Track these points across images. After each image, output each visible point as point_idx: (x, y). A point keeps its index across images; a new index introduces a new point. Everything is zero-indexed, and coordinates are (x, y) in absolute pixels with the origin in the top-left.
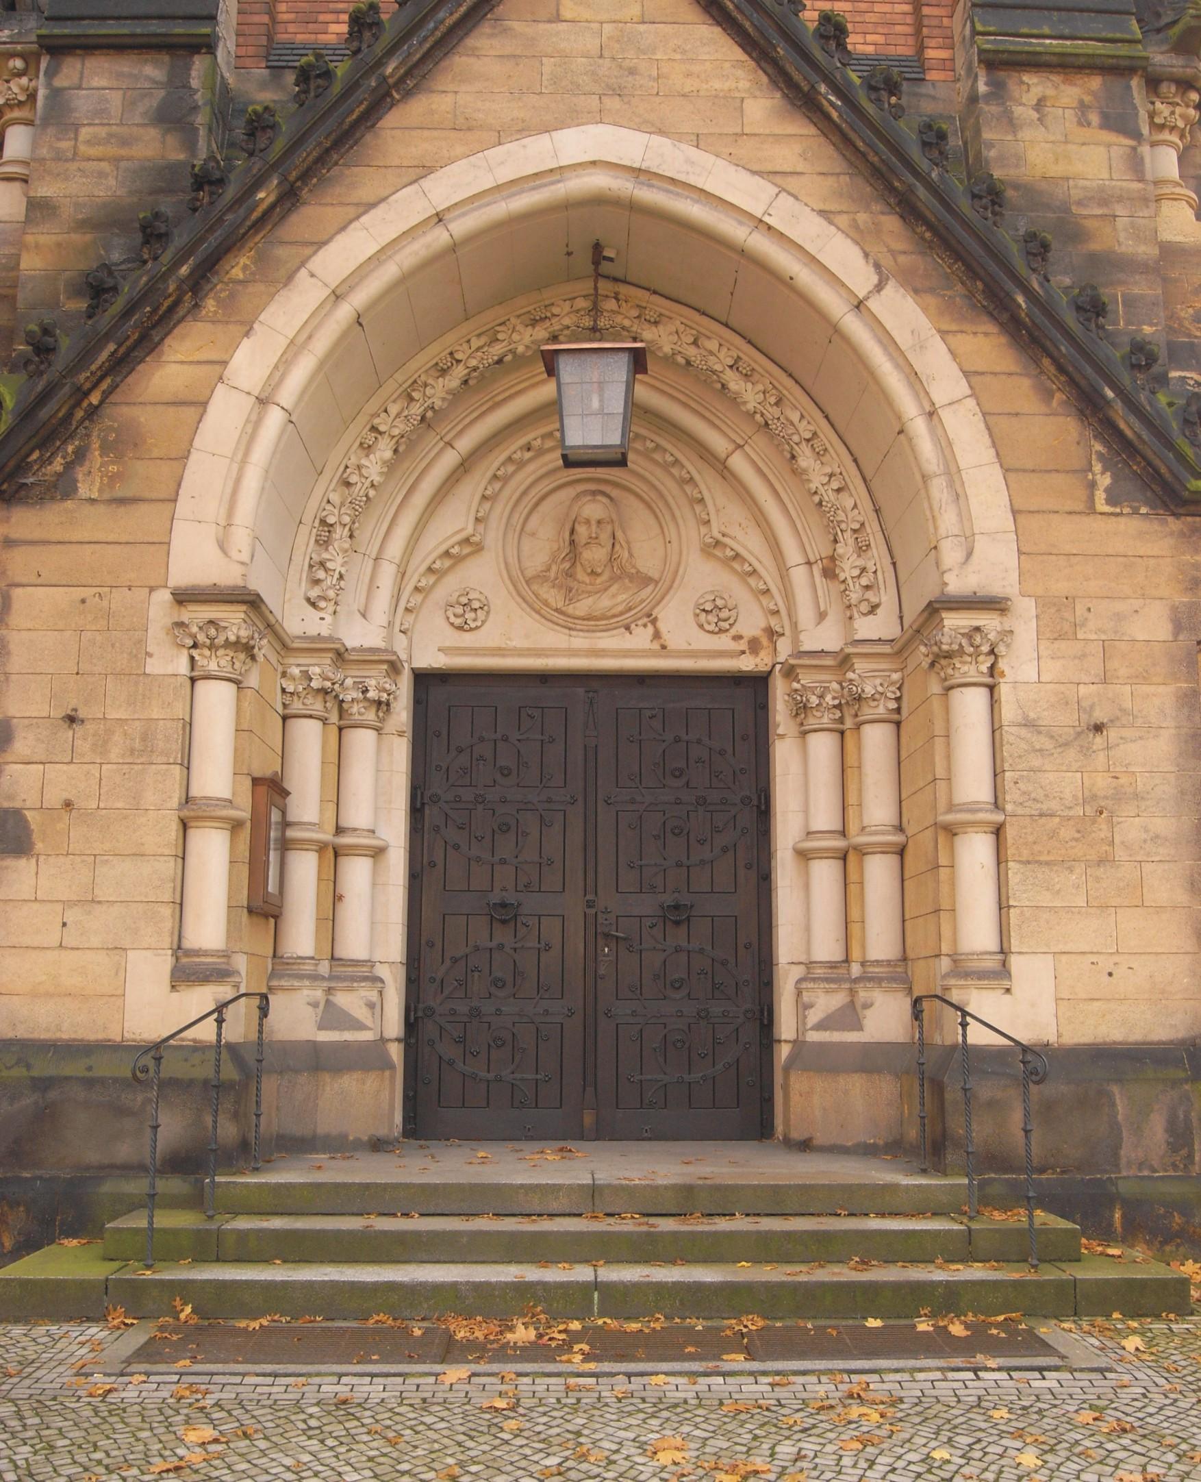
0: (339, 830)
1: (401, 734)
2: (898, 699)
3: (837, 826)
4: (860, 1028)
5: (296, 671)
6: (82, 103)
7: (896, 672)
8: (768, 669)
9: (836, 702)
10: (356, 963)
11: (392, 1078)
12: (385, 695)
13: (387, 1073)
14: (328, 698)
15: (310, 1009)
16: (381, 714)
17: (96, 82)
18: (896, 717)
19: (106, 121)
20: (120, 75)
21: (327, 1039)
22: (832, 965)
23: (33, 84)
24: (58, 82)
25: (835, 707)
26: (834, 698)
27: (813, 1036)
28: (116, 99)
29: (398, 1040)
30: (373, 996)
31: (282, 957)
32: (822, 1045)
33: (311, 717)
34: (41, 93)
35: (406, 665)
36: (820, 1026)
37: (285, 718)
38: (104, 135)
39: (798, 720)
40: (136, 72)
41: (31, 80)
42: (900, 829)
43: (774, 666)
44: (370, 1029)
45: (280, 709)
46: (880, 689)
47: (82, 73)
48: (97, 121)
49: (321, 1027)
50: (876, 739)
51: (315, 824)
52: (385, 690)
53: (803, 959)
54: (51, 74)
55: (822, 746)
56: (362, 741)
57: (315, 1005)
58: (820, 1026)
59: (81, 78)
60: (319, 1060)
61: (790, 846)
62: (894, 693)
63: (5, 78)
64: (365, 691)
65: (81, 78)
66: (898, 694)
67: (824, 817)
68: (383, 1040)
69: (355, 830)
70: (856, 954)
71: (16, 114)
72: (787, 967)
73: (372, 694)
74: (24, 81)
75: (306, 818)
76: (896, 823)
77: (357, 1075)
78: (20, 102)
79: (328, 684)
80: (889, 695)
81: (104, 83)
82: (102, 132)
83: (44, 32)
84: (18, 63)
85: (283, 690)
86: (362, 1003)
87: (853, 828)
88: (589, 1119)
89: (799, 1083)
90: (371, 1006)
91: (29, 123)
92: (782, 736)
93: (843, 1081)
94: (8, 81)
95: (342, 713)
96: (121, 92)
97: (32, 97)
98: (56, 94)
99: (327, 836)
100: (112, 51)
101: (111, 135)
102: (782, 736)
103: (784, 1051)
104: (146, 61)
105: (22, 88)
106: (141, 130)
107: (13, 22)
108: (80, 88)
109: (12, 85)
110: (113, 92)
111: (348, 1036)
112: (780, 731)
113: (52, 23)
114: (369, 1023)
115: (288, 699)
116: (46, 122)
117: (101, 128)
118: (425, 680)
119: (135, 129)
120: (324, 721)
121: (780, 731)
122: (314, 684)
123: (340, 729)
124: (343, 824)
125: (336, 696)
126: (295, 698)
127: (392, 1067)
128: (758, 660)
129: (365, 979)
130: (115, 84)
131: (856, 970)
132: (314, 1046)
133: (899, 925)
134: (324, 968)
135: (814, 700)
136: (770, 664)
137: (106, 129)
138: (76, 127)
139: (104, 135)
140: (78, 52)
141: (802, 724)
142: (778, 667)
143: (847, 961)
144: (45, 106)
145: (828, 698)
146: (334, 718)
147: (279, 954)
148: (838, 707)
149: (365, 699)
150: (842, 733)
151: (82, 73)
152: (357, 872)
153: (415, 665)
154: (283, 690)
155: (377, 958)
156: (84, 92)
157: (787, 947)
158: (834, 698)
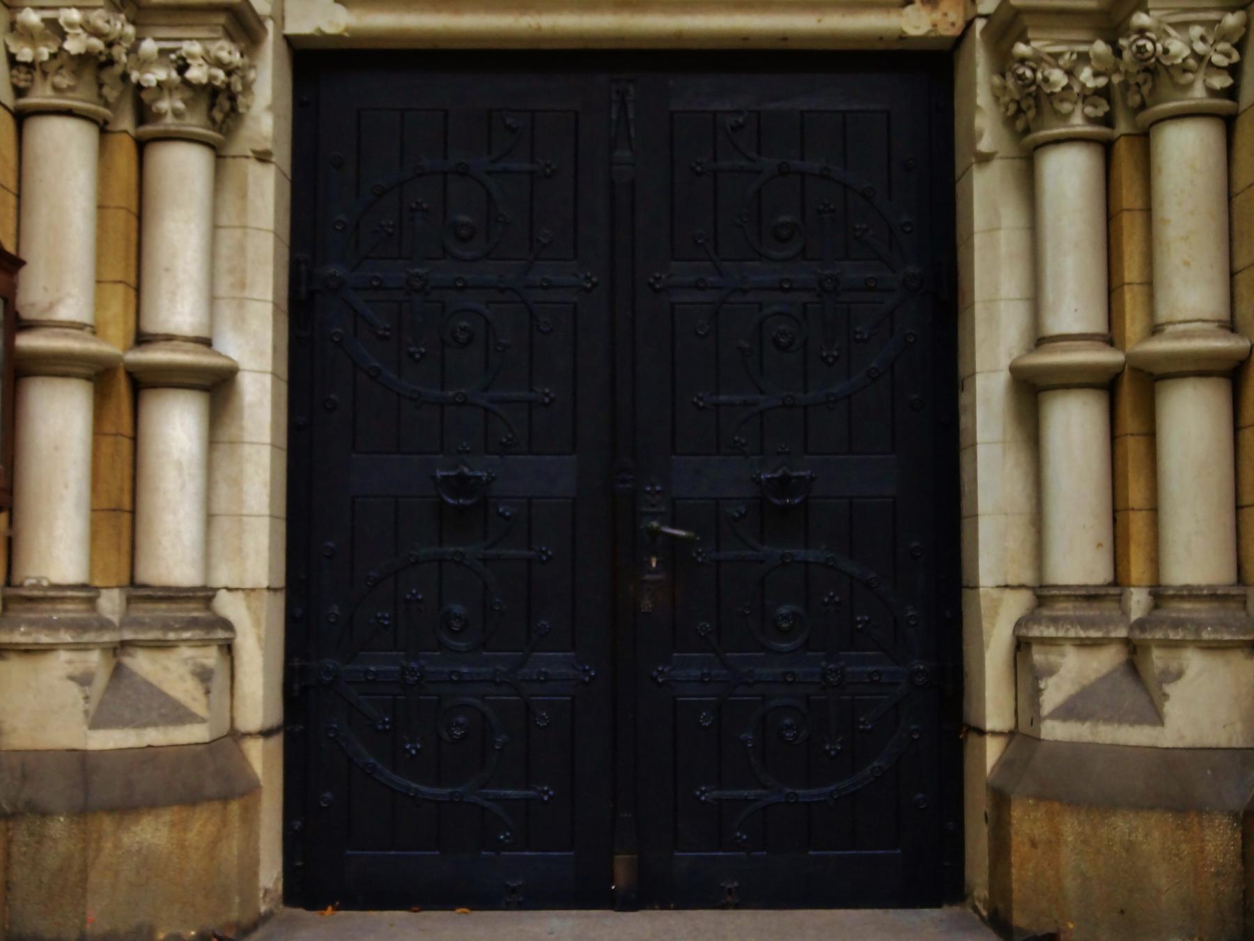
0: (142, 339)
1: (263, 157)
2: (1234, 70)
3: (1094, 322)
4: (1156, 717)
5: (32, 18)
7: (1232, 10)
8: (954, 32)
9: (1102, 81)
10: (174, 595)
11: (249, 818)
12: (221, 74)
13: (235, 807)
14: (106, 76)
15: (74, 690)
16: (218, 116)
18: (1226, 103)
21: (110, 745)
22: (1090, 596)
25: (1098, 92)
26: (1096, 74)
27: (1054, 731)
29: (266, 733)
30: (211, 657)
31: (21, 586)
32: (1076, 748)
33: (68, 113)
35: (270, 25)
36: (1067, 711)
37: (21, 117)
39: (1020, 124)
42: (1231, 326)
43: (969, 24)
44: (203, 721)
45: (9, 100)
46: (1200, 47)
49: (97, 722)
50: (1185, 151)
51: (81, 326)
52: (219, 63)
53: (1027, 577)
55: (1069, 174)
56: (183, 169)
57: (84, 680)
58: (1067, 711)
60: (100, 790)
61: (1005, 362)
62: (1228, 55)
64: (183, 67)
66: (1236, 57)
67: (1074, 307)
68: (236, 735)
69: (169, 338)
70: (1138, 569)
72: (996, 593)
73: (197, 73)
75: (65, 313)
76: (1224, 314)
77: (167, 816)
79: (98, 44)
80: (1217, 59)
85: (12, 61)
86: (184, 670)
87: (1133, 325)
88: (623, 871)
89: (1026, 821)
90: (204, 676)
92: (985, 159)
93: (1122, 825)
95: (143, 113)
99: (112, 346)
102: (985, 159)
103: (993, 750)
111: (154, 736)
112: (984, 145)
114: (199, 708)
115: (22, 79)
118: (312, 62)
120: (104, 129)
121: (984, 145)
122: (73, 46)
123: (142, 146)
124: (150, 327)
125: (125, 77)
126: (37, 75)
127: (251, 790)
128: (937, 16)
129: (192, 624)
131: (1138, 602)
132: (83, 760)
133: (1228, 518)
134: (111, 603)
135: (1058, 78)
136: (960, 23)
141: (1027, 131)
142: (980, 24)
143: (1119, 580)
145: (1086, 74)
146: (126, 123)
147: (16, 580)
148: (1104, 93)
149: (186, 83)
150: (1107, 148)
152: (177, 425)
153: (292, 28)
154: (12, 61)
155: (222, 577)
157: (995, 552)
158: (1096, 74)
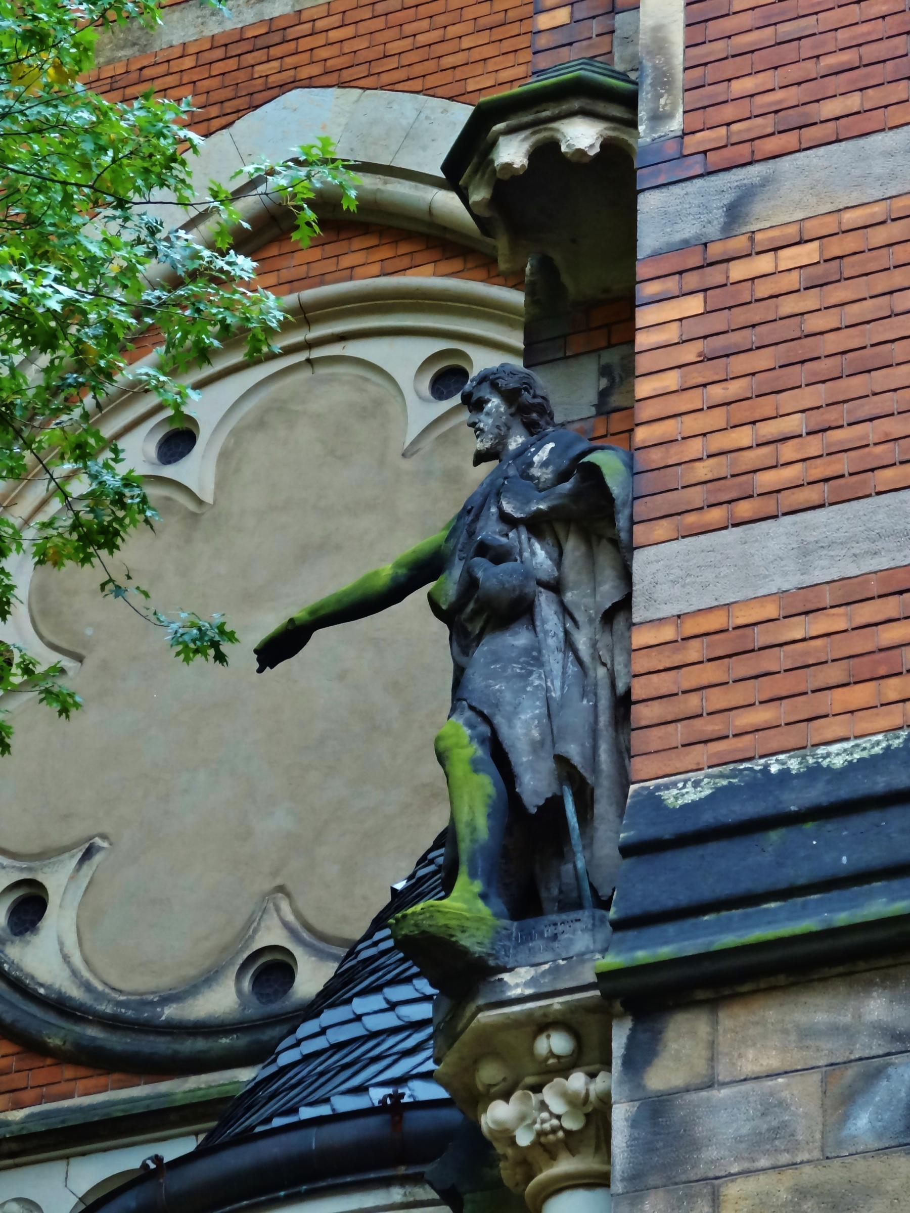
6: (723, 1124)
17: (753, 1061)
19: (785, 1158)
23: (599, 1084)
24: (660, 1077)
28: (802, 1097)
34: (620, 1115)
38: (784, 1196)
40: (846, 1018)
41: (592, 1076)
47: (712, 1045)
48: (763, 1162)
54: (639, 1058)
59: (712, 1059)
63: (530, 1080)
65: (712, 1059)
71: (565, 1165)
74: (577, 1081)
78: (568, 1133)
81: (772, 1061)
82: (779, 1187)
83: (612, 961)
84: (558, 1043)
91: (598, 1181)
94: (537, 1089)
96: (815, 1078)
97: (597, 1116)
98: (656, 1110)
100: (782, 979)
101: (801, 1193)
104: (869, 985)
106: (877, 1166)
107: (538, 943)
108: (711, 1084)
109: (548, 1095)
110: (797, 1078)
113: (631, 934)
116: (639, 1184)
117: (773, 1176)
119: (860, 1165)
130: (796, 1059)
137: (789, 1178)
138: (713, 1185)
139: (784, 1196)
140: (700, 995)
144: (633, 1144)
151: (712, 1045)
156: (724, 1092)
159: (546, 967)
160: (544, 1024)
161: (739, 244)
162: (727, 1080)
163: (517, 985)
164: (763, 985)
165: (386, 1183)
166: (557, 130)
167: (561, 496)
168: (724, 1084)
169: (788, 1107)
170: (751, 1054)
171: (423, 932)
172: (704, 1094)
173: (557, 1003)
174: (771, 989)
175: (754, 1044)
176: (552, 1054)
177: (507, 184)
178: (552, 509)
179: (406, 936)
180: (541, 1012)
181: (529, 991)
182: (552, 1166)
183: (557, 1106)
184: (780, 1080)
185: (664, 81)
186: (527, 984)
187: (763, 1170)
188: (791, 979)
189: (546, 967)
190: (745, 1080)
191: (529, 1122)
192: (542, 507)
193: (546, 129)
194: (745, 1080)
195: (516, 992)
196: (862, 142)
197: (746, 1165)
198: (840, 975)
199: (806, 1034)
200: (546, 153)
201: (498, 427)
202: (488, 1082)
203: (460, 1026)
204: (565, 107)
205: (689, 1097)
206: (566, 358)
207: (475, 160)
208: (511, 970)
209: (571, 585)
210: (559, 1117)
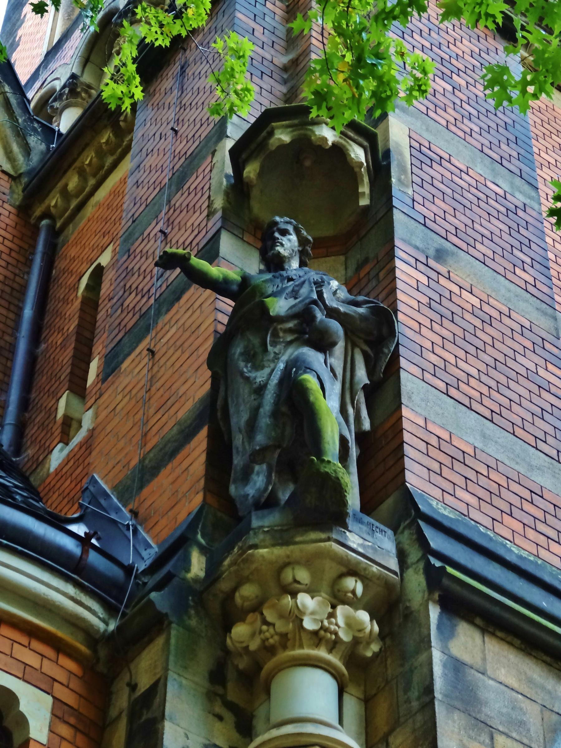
19: (525, 741)
20: (530, 681)
40: (549, 687)
47: (483, 651)
48: (514, 735)
71: (322, 653)
81: (512, 682)
100: (517, 642)
105: (350, 624)
151: (483, 651)
159: (370, 544)
160: (353, 571)
161: (443, 269)
162: (492, 676)
163: (354, 542)
164: (509, 639)
165: (67, 579)
166: (351, 146)
167: (355, 312)
168: (490, 678)
169: (524, 714)
170: (503, 671)
171: (338, 478)
172: (480, 675)
173: (375, 568)
174: (510, 644)
175: (504, 667)
176: (354, 592)
177: (305, 146)
178: (345, 314)
179: (327, 473)
180: (364, 566)
181: (361, 550)
182: (313, 649)
183: (341, 621)
184: (520, 696)
185: (402, 169)
186: (358, 544)
187: (512, 737)
188: (523, 646)
189: (370, 544)
190: (501, 683)
191: (317, 617)
192: (342, 309)
193: (345, 140)
194: (501, 683)
195: (354, 546)
196: (495, 274)
197: (506, 731)
198: (544, 662)
199: (530, 681)
200: (338, 151)
201: (293, 250)
202: (298, 578)
203: (298, 539)
204: (360, 140)
205: (473, 671)
206: (242, 239)
207: (296, 121)
208: (350, 531)
209: (336, 356)
210: (339, 627)
